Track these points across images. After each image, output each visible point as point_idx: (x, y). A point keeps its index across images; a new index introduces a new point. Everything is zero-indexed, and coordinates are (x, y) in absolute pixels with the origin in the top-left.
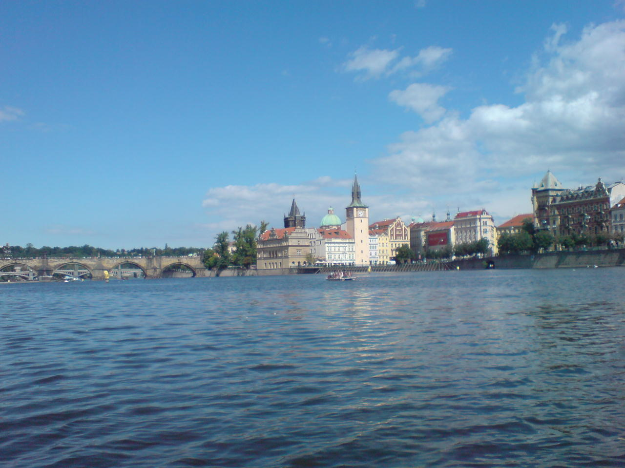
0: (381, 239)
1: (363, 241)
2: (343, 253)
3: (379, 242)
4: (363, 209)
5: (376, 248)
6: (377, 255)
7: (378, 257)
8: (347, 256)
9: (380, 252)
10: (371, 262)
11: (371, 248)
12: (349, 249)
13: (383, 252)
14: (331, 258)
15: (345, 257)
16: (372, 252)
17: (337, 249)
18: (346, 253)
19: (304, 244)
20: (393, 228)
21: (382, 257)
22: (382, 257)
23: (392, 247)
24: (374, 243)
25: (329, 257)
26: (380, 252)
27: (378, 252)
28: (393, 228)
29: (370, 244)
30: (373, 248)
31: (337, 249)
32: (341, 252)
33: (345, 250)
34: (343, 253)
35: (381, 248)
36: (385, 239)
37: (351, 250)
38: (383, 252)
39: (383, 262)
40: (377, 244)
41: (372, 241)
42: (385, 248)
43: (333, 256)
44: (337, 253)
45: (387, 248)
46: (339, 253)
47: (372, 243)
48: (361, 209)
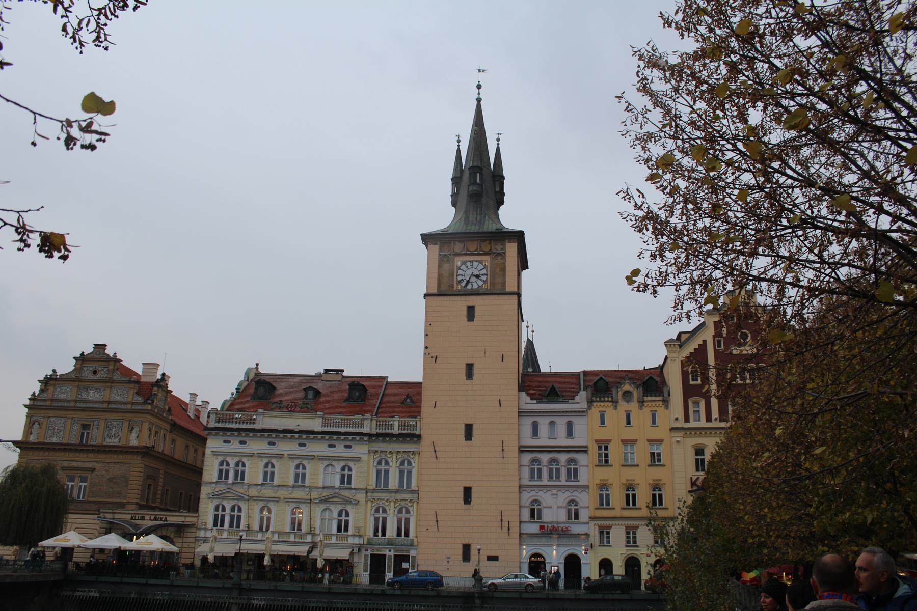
0: (614, 415)
1: (475, 432)
2: (325, 500)
3: (602, 434)
4: (486, 247)
5: (573, 474)
6: (584, 515)
7: (593, 530)
8: (362, 520)
9: (604, 501)
10: (537, 565)
11: (535, 474)
12: (382, 476)
13: (631, 501)
14: (235, 522)
15: (343, 527)
16: (546, 498)
17: (285, 473)
18: (348, 501)
19: (114, 441)
20: (703, 346)
21: (618, 534)
22: (618, 534)
23: (699, 465)
24: (562, 440)
25: (218, 522)
26: (604, 501)
27: (587, 501)
28: (703, 346)
29: (522, 450)
30: (554, 474)
31: (285, 473)
32: (314, 494)
33: (346, 479)
34: (325, 500)
35: (615, 476)
36: (641, 416)
37: (393, 483)
38: (631, 501)
39: (632, 564)
40: (583, 450)
41: (543, 429)
42: (643, 477)
43: (251, 515)
44: (283, 493)
45: (656, 473)
46: (299, 494)
47: (543, 440)
48: (473, 246)
